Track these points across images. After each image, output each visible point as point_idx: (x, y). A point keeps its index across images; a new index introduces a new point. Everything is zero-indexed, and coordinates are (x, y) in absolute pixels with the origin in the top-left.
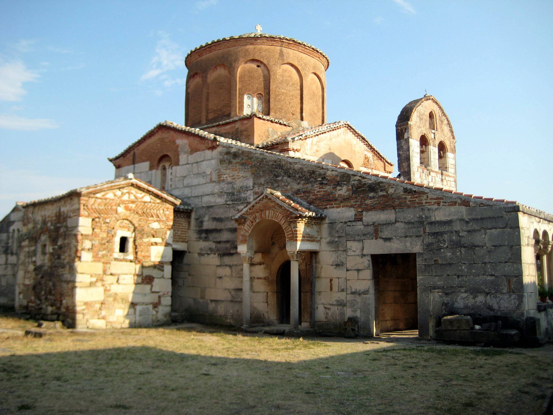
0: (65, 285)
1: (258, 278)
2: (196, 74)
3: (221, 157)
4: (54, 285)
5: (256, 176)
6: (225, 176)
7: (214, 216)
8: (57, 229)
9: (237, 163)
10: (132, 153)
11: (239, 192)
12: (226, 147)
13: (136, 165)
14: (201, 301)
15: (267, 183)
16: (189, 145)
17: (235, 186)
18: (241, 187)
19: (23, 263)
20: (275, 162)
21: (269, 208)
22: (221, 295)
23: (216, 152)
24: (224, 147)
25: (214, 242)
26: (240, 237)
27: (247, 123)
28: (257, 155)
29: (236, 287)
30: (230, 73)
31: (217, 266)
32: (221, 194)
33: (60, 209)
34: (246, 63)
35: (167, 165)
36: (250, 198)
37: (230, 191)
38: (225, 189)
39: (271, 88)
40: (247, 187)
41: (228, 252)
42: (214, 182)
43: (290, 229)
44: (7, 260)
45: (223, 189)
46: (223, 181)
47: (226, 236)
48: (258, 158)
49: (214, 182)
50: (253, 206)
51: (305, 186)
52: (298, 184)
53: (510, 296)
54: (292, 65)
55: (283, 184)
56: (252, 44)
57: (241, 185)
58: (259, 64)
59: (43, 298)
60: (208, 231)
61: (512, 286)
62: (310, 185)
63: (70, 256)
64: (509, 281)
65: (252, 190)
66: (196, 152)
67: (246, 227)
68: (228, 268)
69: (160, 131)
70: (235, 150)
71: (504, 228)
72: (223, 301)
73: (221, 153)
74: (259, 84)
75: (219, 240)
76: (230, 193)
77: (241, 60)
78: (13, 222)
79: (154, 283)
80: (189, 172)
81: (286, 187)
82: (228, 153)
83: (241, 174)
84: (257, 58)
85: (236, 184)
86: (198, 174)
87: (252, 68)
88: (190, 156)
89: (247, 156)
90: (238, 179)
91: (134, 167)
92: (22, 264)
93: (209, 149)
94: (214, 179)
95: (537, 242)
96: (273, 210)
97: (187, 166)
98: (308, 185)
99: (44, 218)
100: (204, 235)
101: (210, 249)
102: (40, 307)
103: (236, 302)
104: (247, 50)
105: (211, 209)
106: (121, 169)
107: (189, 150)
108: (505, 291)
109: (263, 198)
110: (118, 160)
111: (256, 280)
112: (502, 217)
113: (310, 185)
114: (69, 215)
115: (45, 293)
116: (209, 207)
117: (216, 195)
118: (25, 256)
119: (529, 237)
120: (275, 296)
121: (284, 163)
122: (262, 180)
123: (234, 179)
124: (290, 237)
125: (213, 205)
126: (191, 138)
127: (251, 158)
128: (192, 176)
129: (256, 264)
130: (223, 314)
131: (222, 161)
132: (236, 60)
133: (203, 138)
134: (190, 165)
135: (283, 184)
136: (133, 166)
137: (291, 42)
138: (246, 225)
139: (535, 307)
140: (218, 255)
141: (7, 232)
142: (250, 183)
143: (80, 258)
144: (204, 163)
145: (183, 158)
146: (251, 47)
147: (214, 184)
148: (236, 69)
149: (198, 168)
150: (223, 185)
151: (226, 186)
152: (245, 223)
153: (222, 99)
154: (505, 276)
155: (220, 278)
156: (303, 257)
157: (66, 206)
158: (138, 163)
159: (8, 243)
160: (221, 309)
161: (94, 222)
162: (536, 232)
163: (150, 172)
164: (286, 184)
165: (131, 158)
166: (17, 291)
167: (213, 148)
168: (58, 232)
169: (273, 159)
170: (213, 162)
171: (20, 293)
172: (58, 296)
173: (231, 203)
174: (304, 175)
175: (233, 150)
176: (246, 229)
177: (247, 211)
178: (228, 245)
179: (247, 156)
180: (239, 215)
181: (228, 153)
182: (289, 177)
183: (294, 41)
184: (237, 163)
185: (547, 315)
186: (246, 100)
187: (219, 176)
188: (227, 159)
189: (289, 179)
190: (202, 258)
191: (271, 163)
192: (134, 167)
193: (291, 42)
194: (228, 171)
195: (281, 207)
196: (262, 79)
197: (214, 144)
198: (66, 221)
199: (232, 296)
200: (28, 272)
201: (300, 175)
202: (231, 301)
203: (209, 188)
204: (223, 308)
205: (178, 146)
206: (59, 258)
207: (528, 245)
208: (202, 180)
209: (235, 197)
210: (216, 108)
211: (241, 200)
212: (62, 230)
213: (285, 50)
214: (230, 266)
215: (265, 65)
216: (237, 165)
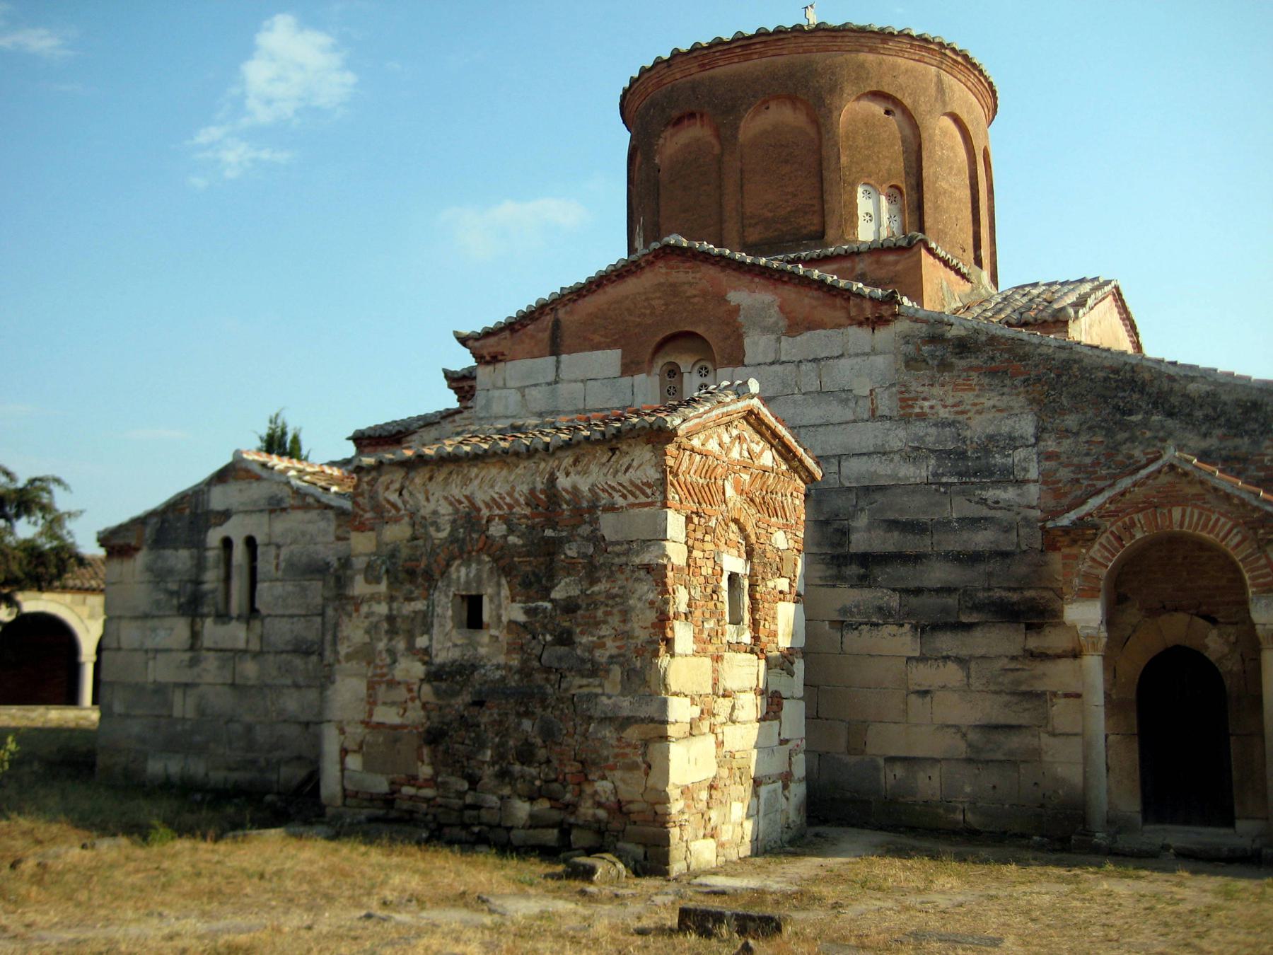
0: (608, 733)
1: (1066, 695)
2: (692, 115)
3: (910, 349)
4: (548, 733)
5: (1045, 408)
6: (926, 404)
7: (891, 515)
8: (550, 549)
9: (971, 368)
10: (548, 320)
11: (987, 452)
12: (923, 321)
13: (564, 357)
14: (852, 760)
15: (1090, 428)
16: (781, 308)
17: (968, 433)
18: (991, 438)
19: (365, 654)
20: (1116, 371)
21: (1183, 501)
22: (925, 743)
23: (884, 335)
24: (917, 321)
25: (894, 590)
26: (1076, 581)
27: (896, 263)
28: (1044, 350)
29: (984, 722)
30: (815, 122)
31: (909, 659)
32: (914, 454)
33: (552, 480)
34: (858, 99)
35: (685, 362)
36: (1026, 470)
37: (950, 446)
38: (930, 439)
39: (925, 174)
40: (1013, 439)
41: (952, 620)
42: (883, 418)
43: (1263, 562)
44: (195, 635)
45: (921, 439)
46: (921, 416)
47: (938, 574)
48: (1049, 358)
49: (883, 418)
50: (1123, 494)
51: (1230, 443)
52: (1205, 436)
54: (956, 119)
55: (1148, 434)
56: (872, 50)
57: (990, 430)
58: (890, 107)
59: (488, 772)
60: (868, 560)
62: (1246, 439)
63: (627, 635)
65: (1033, 446)
66: (809, 329)
67: (1096, 551)
68: (952, 667)
69: (661, 264)
70: (963, 333)
72: (935, 761)
73: (907, 339)
74: (893, 161)
75: (913, 584)
76: (949, 452)
77: (849, 89)
78: (226, 515)
79: (783, 714)
80: (784, 384)
81: (1159, 444)
82: (934, 339)
83: (990, 400)
84: (886, 89)
85: (969, 427)
86: (820, 392)
87: (874, 115)
88: (786, 342)
89: (1009, 351)
90: (979, 412)
91: (558, 362)
92: (349, 657)
93: (860, 324)
94: (883, 409)
96: (1195, 506)
97: (777, 368)
98: (1238, 441)
99: (464, 507)
100: (854, 570)
101: (880, 609)
102: (469, 799)
103: (987, 762)
104: (861, 66)
105: (879, 497)
106: (500, 366)
107: (783, 323)
109: (1159, 471)
110: (492, 340)
111: (1061, 702)
113: (1246, 439)
114: (604, 499)
115: (500, 757)
116: (867, 490)
117: (897, 458)
118: (372, 630)
120: (1136, 746)
121: (1147, 376)
122: (1071, 421)
123: (963, 412)
124: (1265, 584)
125: (882, 483)
126: (789, 292)
127: (1025, 357)
128: (799, 397)
129: (1059, 657)
130: (937, 798)
131: (912, 362)
132: (834, 88)
133: (846, 294)
134: (791, 367)
135: (1148, 434)
136: (551, 360)
137: (959, 59)
138: (1097, 546)
140: (914, 627)
141: (198, 545)
142: (1026, 426)
143: (669, 643)
144: (843, 361)
145: (756, 345)
146: (871, 57)
147: (888, 424)
148: (835, 114)
149: (820, 376)
150: (919, 428)
151: (933, 431)
152: (1093, 539)
153: (790, 189)
155: (924, 693)
156: (1232, 638)
157: (585, 472)
158: (569, 353)
159: (198, 582)
160: (928, 785)
161: (691, 526)
163: (627, 380)
164: (1161, 434)
165: (546, 336)
166: (331, 744)
167: (876, 322)
168: (551, 554)
169: (1107, 364)
170: (880, 361)
171: (344, 752)
172: (571, 768)
173: (954, 479)
174: (1223, 413)
175: (953, 332)
176: (1099, 557)
177: (1100, 507)
178: (951, 601)
179: (1009, 351)
180: (1072, 516)
181: (934, 339)
182: (1170, 415)
183: (966, 57)
184: (971, 368)
186: (864, 204)
187: (906, 401)
188: (934, 357)
189: (1169, 423)
190: (851, 638)
191: (1101, 374)
192: (558, 362)
193: (959, 59)
194: (937, 390)
195: (1228, 497)
196: (898, 147)
197: (885, 311)
198: (594, 521)
199: (970, 745)
200: (393, 684)
201: (1210, 411)
202: (969, 760)
203: (868, 435)
204: (936, 779)
205: (737, 309)
206: (565, 639)
208: (837, 412)
209: (971, 465)
210: (770, 215)
211: (992, 474)
212: (571, 551)
213: (947, 78)
214: (961, 661)
215: (905, 110)
216: (974, 375)
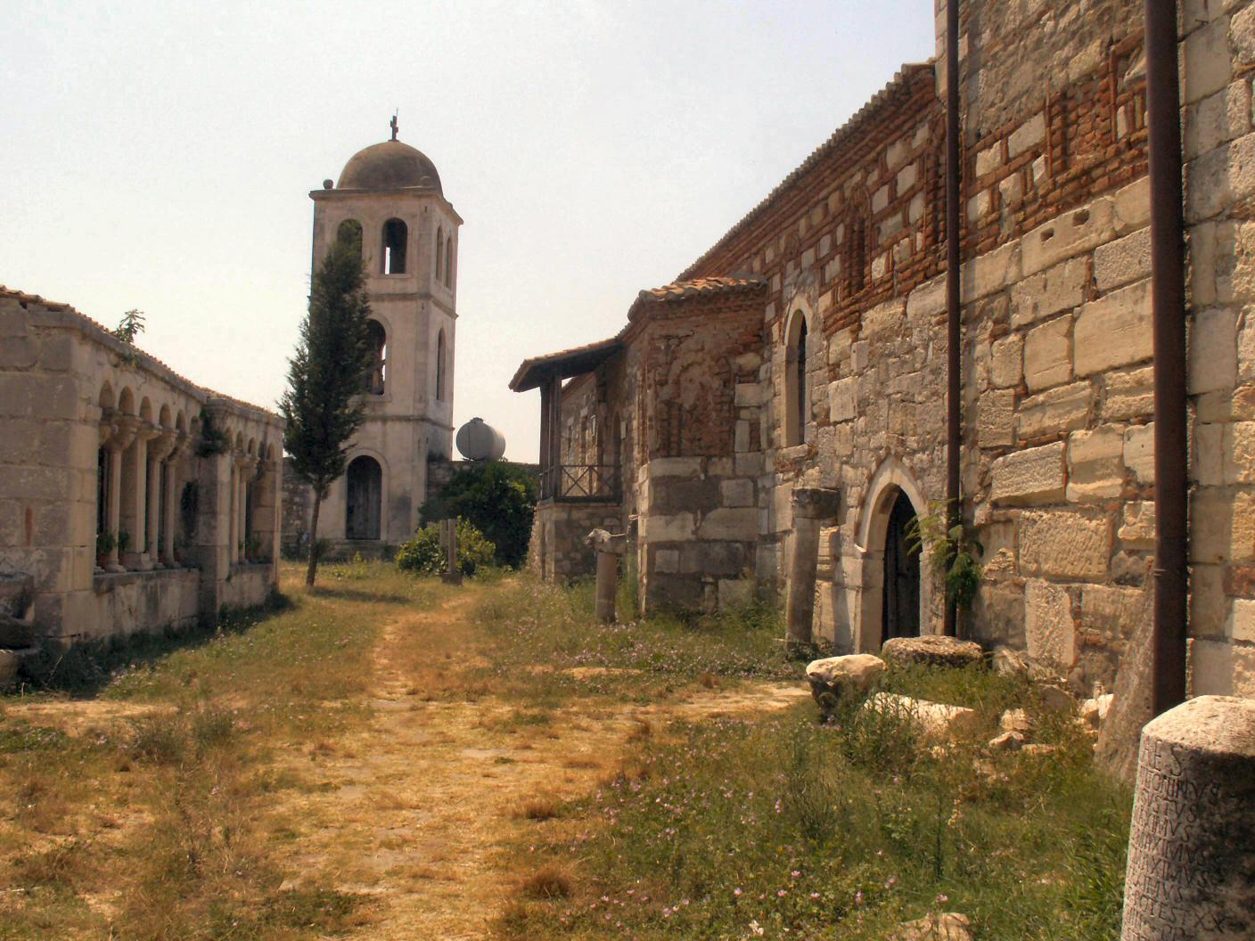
53: (28, 554)
61: (36, 529)
64: (29, 513)
71: (27, 369)
95: (107, 415)
108: (13, 541)
112: (23, 338)
119: (88, 401)
139: (89, 583)
154: (18, 499)
162: (107, 390)
185: (112, 602)
207: (85, 421)
